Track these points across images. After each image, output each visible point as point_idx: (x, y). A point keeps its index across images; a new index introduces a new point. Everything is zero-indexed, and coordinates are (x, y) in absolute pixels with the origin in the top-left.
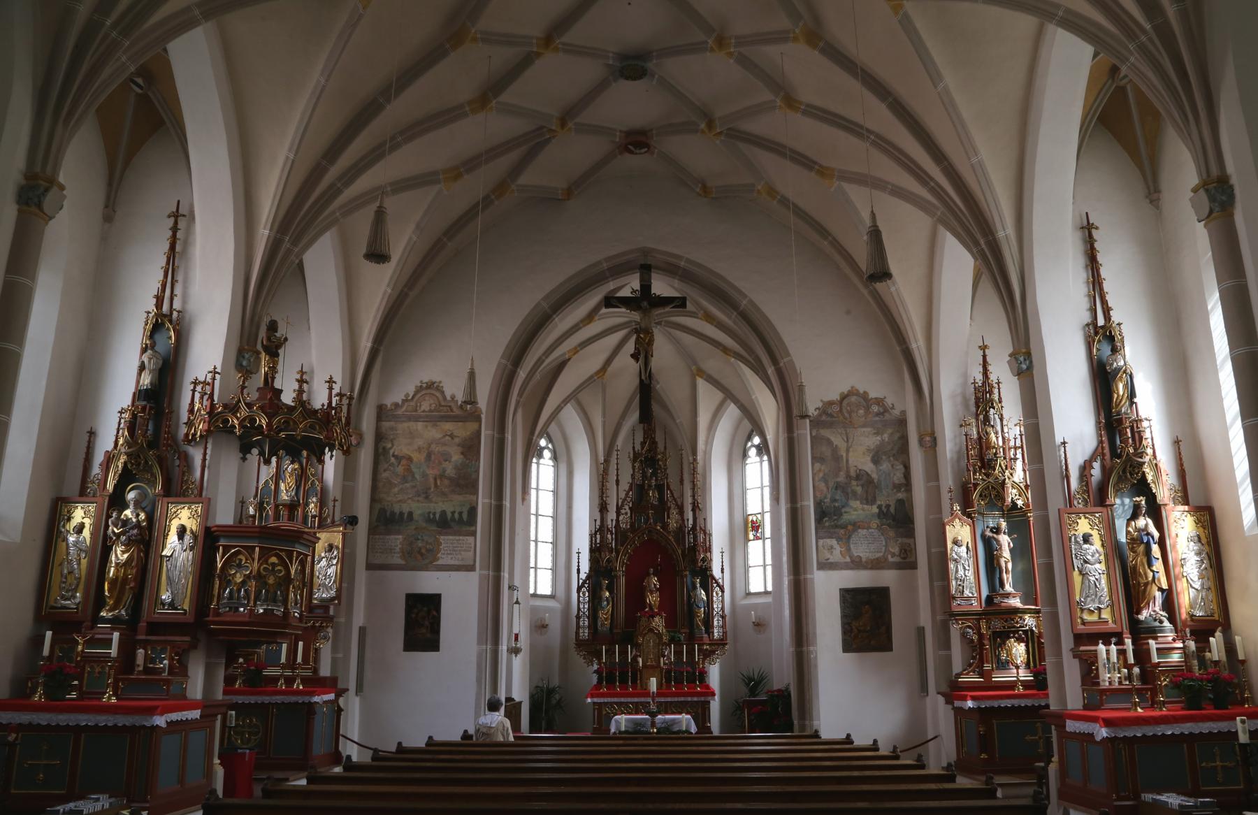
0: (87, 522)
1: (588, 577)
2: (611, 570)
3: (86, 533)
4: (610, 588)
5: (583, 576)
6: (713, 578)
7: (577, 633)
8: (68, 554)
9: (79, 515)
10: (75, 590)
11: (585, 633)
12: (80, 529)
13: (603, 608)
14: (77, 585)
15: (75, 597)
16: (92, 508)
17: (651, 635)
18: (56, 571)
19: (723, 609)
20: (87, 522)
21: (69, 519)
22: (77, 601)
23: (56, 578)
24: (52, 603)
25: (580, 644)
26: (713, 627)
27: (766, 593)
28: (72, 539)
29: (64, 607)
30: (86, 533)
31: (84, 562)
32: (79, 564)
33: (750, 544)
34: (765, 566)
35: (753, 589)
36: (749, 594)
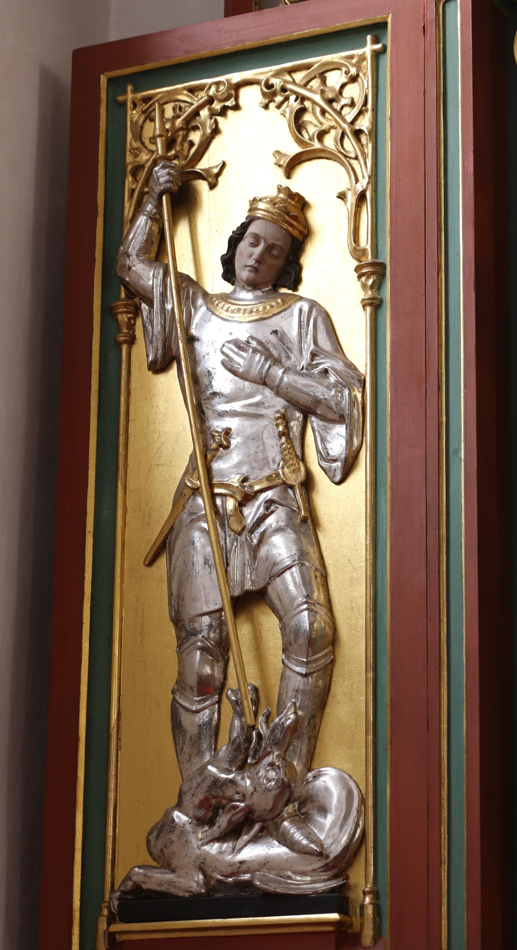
0: (324, 186)
3: (331, 274)
8: (210, 444)
9: (248, 152)
10: (306, 735)
12: (275, 255)
14: (320, 700)
15: (300, 802)
16: (346, 76)
18: (140, 598)
20: (324, 186)
21: (183, 200)
22: (331, 830)
23: (144, 661)
24: (129, 862)
28: (221, 333)
29: (242, 894)
30: (331, 274)
31: (345, 508)
32: (307, 523)
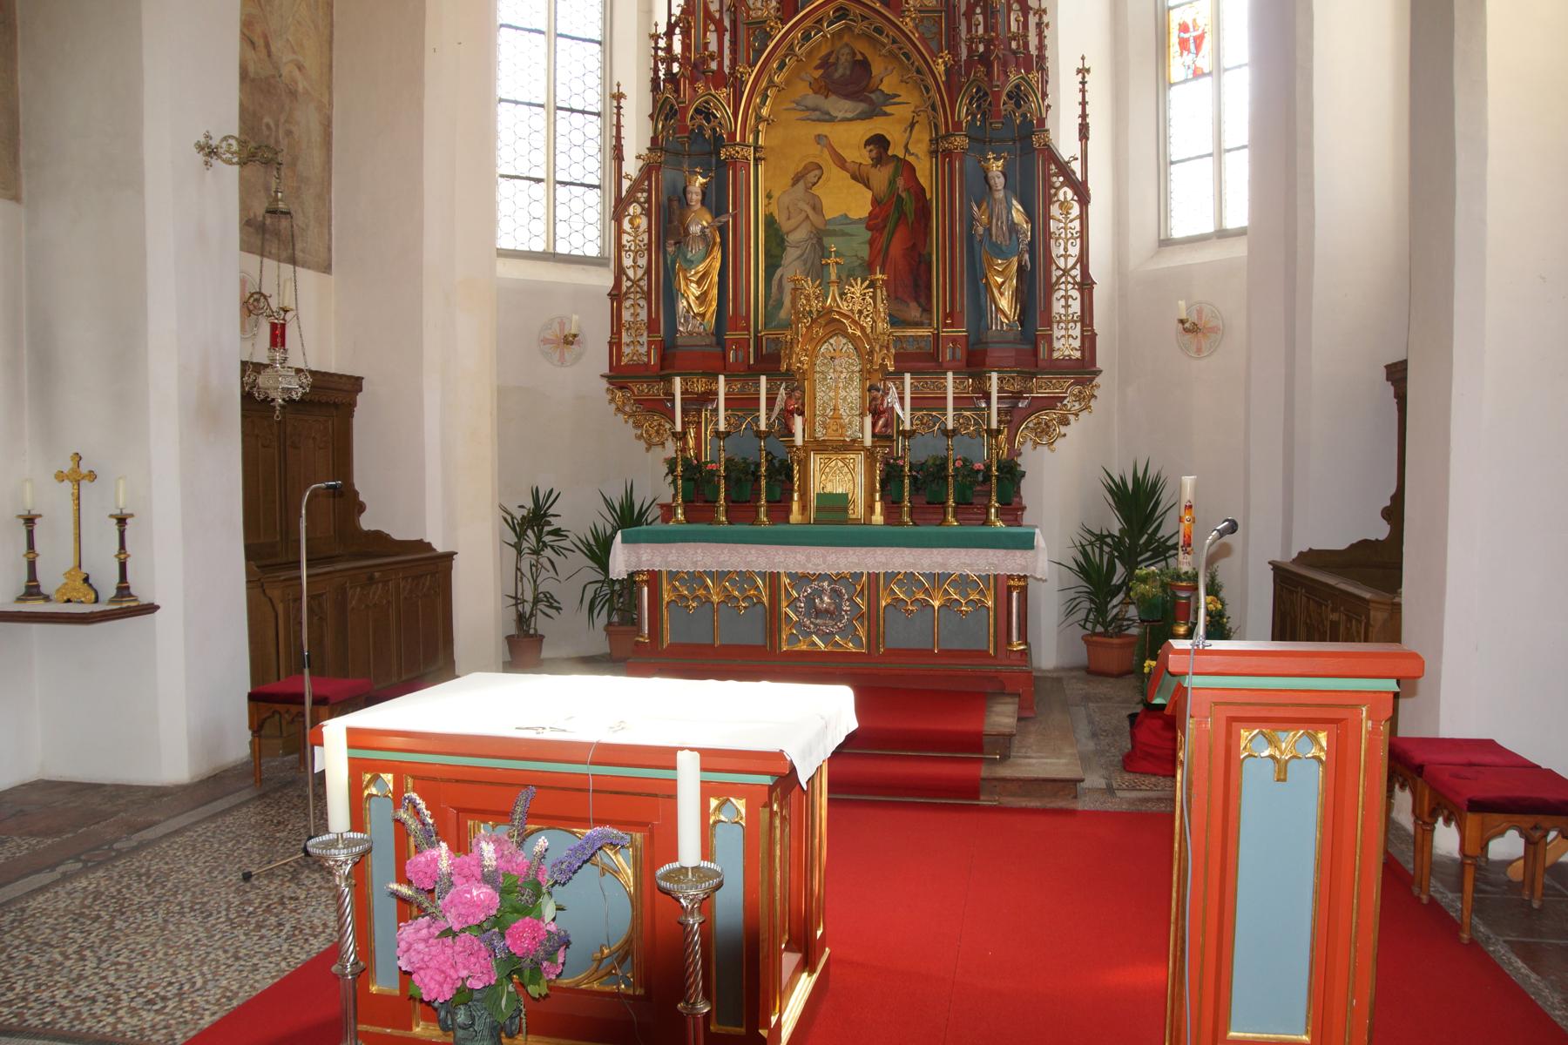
1: (648, 170)
2: (718, 142)
4: (715, 201)
5: (631, 167)
6: (1051, 155)
7: (615, 344)
11: (638, 348)
13: (691, 263)
17: (838, 342)
19: (1083, 259)
25: (620, 376)
26: (1049, 322)
27: (1222, 234)
33: (1174, 93)
34: (1219, 153)
35: (1179, 230)
36: (1166, 243)
